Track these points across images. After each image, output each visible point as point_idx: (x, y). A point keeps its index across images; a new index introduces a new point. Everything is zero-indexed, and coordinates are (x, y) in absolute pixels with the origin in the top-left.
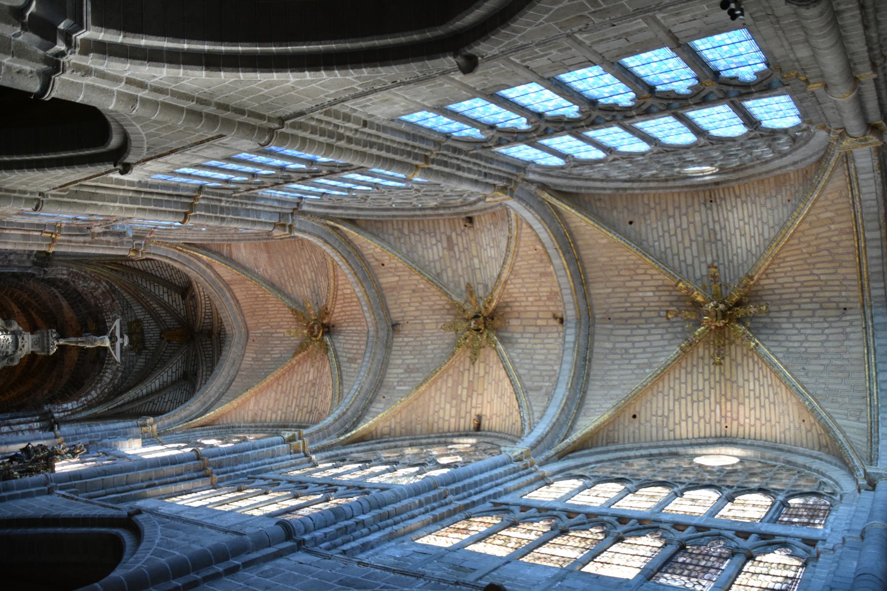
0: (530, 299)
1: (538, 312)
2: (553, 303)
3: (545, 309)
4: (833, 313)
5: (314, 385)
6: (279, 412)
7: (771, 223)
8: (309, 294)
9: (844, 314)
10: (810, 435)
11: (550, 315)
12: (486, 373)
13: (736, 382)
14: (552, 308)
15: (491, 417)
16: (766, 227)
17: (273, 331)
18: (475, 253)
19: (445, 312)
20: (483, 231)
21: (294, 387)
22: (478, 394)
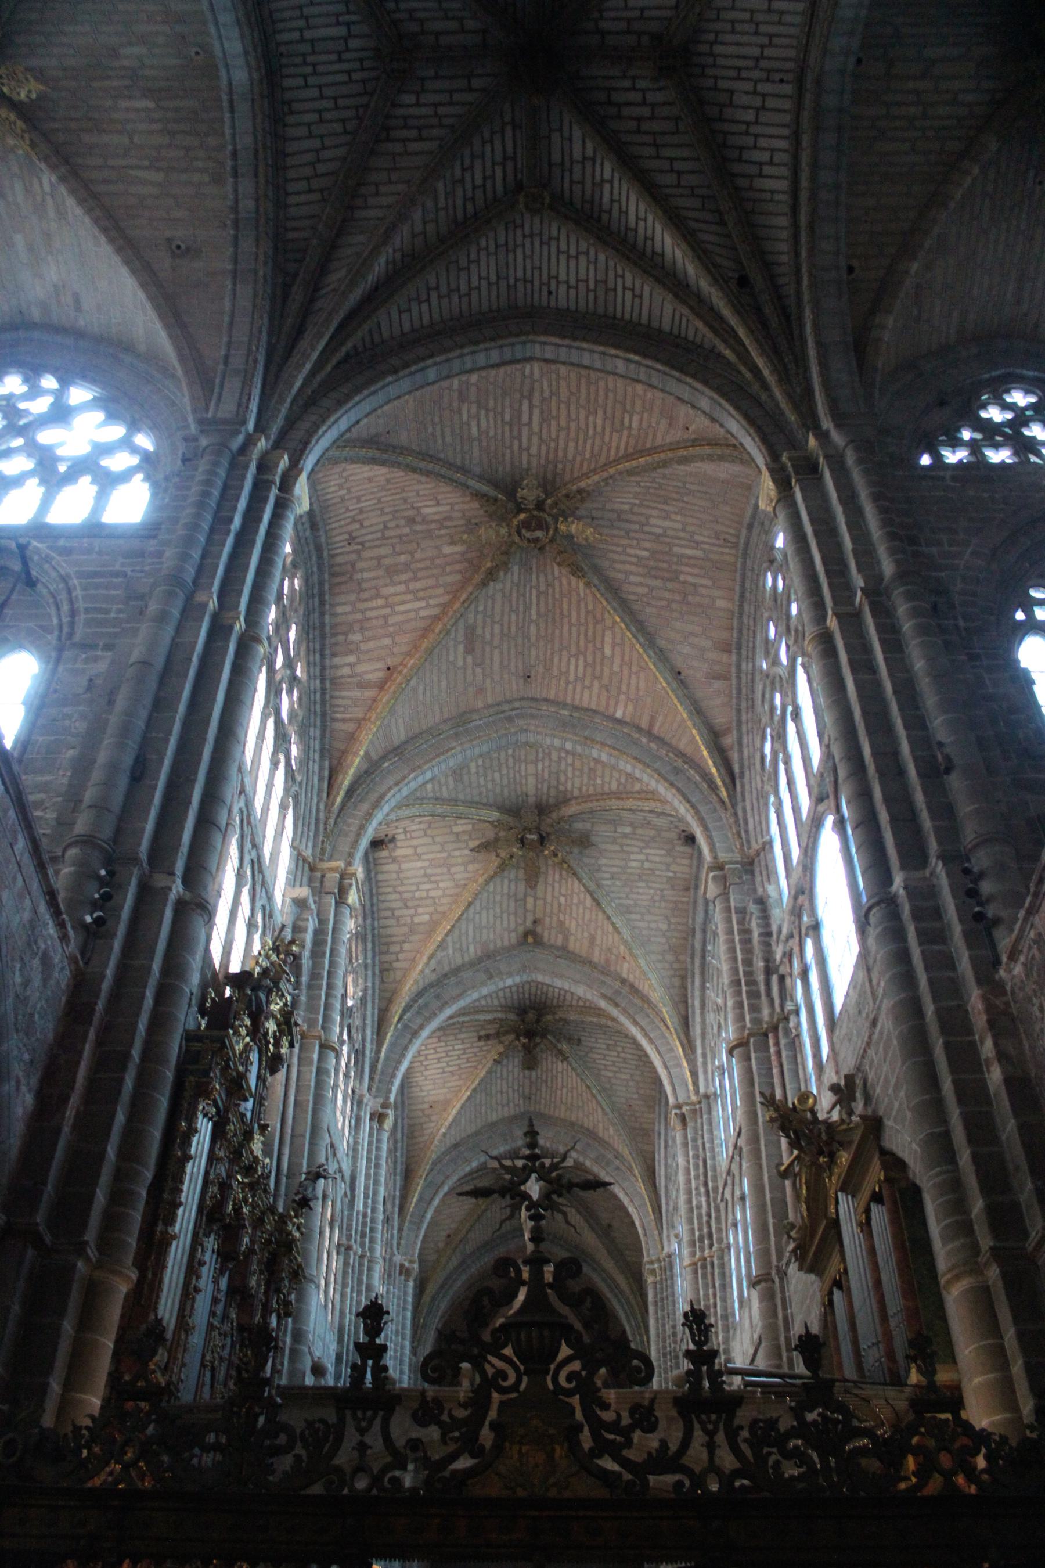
0: (562, 900)
1: (545, 899)
2: (554, 925)
3: (548, 910)
4: (527, 1091)
5: (411, 521)
6: (344, 492)
7: (614, 1081)
8: (617, 506)
9: (524, 1098)
10: (420, 1114)
11: (539, 915)
12: (457, 834)
13: (461, 1032)
14: (547, 920)
15: (395, 860)
16: (610, 1074)
17: (536, 401)
18: (640, 831)
19: (554, 783)
20: (669, 853)
21: (403, 491)
22: (425, 830)
